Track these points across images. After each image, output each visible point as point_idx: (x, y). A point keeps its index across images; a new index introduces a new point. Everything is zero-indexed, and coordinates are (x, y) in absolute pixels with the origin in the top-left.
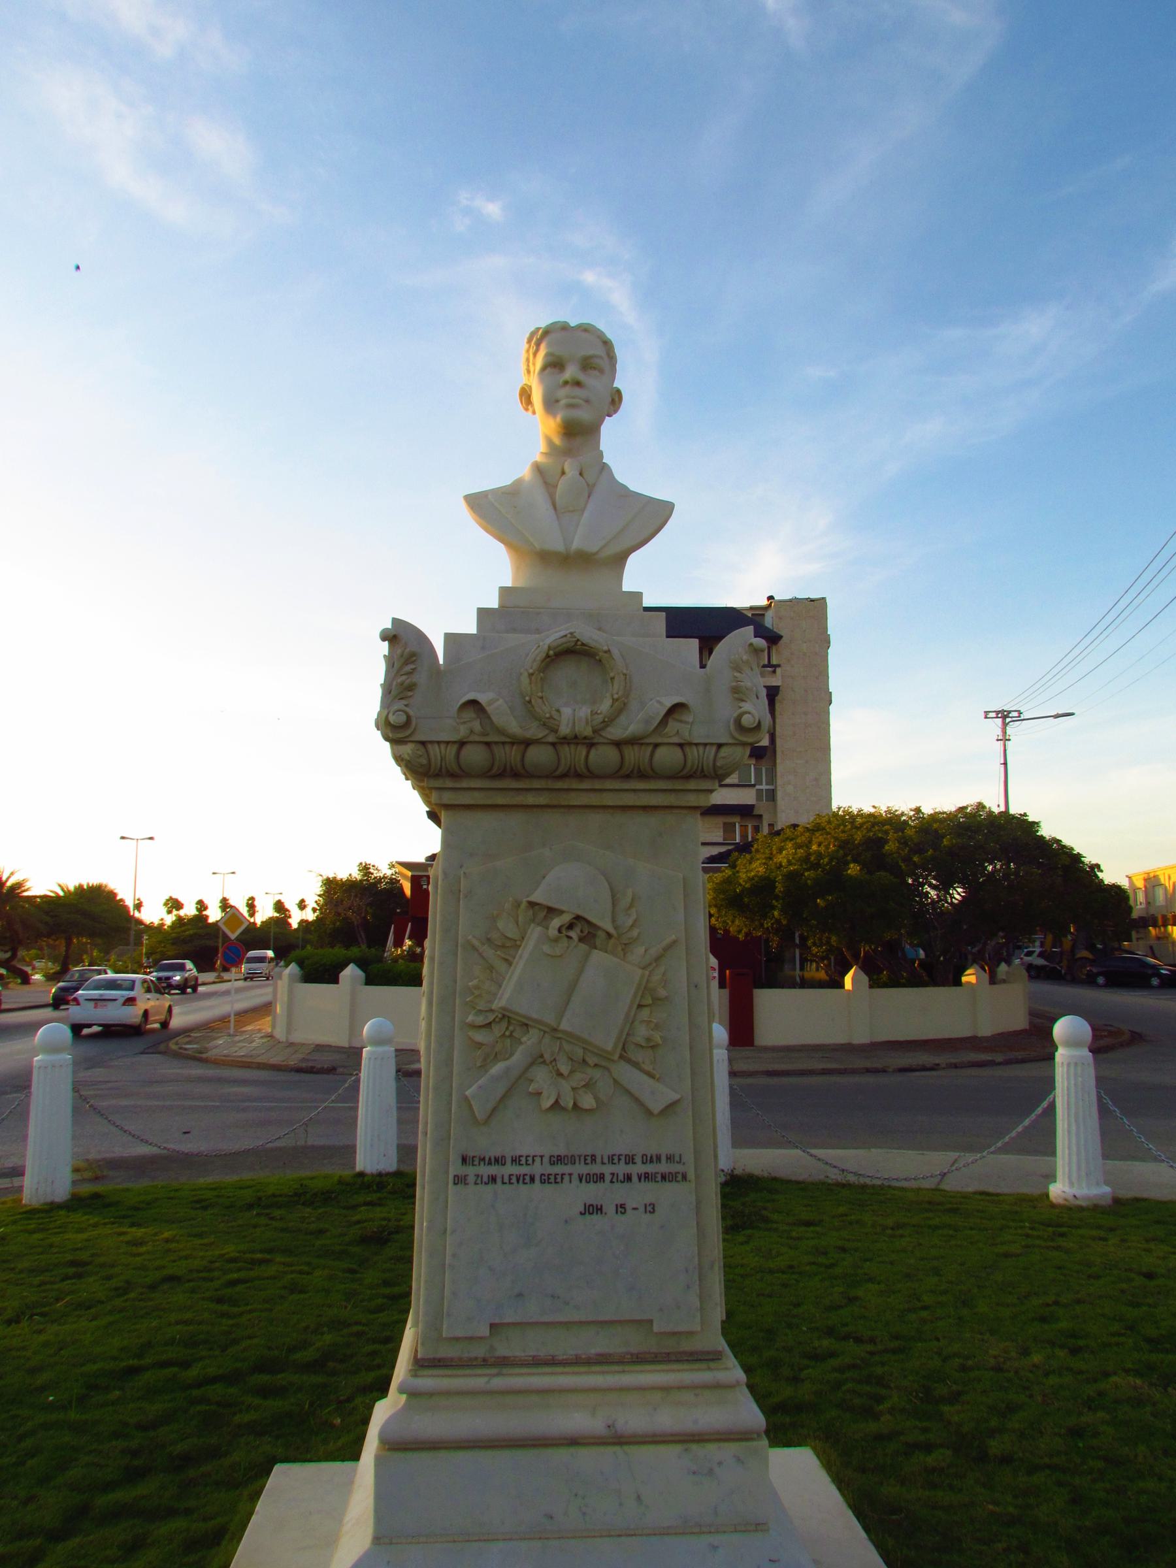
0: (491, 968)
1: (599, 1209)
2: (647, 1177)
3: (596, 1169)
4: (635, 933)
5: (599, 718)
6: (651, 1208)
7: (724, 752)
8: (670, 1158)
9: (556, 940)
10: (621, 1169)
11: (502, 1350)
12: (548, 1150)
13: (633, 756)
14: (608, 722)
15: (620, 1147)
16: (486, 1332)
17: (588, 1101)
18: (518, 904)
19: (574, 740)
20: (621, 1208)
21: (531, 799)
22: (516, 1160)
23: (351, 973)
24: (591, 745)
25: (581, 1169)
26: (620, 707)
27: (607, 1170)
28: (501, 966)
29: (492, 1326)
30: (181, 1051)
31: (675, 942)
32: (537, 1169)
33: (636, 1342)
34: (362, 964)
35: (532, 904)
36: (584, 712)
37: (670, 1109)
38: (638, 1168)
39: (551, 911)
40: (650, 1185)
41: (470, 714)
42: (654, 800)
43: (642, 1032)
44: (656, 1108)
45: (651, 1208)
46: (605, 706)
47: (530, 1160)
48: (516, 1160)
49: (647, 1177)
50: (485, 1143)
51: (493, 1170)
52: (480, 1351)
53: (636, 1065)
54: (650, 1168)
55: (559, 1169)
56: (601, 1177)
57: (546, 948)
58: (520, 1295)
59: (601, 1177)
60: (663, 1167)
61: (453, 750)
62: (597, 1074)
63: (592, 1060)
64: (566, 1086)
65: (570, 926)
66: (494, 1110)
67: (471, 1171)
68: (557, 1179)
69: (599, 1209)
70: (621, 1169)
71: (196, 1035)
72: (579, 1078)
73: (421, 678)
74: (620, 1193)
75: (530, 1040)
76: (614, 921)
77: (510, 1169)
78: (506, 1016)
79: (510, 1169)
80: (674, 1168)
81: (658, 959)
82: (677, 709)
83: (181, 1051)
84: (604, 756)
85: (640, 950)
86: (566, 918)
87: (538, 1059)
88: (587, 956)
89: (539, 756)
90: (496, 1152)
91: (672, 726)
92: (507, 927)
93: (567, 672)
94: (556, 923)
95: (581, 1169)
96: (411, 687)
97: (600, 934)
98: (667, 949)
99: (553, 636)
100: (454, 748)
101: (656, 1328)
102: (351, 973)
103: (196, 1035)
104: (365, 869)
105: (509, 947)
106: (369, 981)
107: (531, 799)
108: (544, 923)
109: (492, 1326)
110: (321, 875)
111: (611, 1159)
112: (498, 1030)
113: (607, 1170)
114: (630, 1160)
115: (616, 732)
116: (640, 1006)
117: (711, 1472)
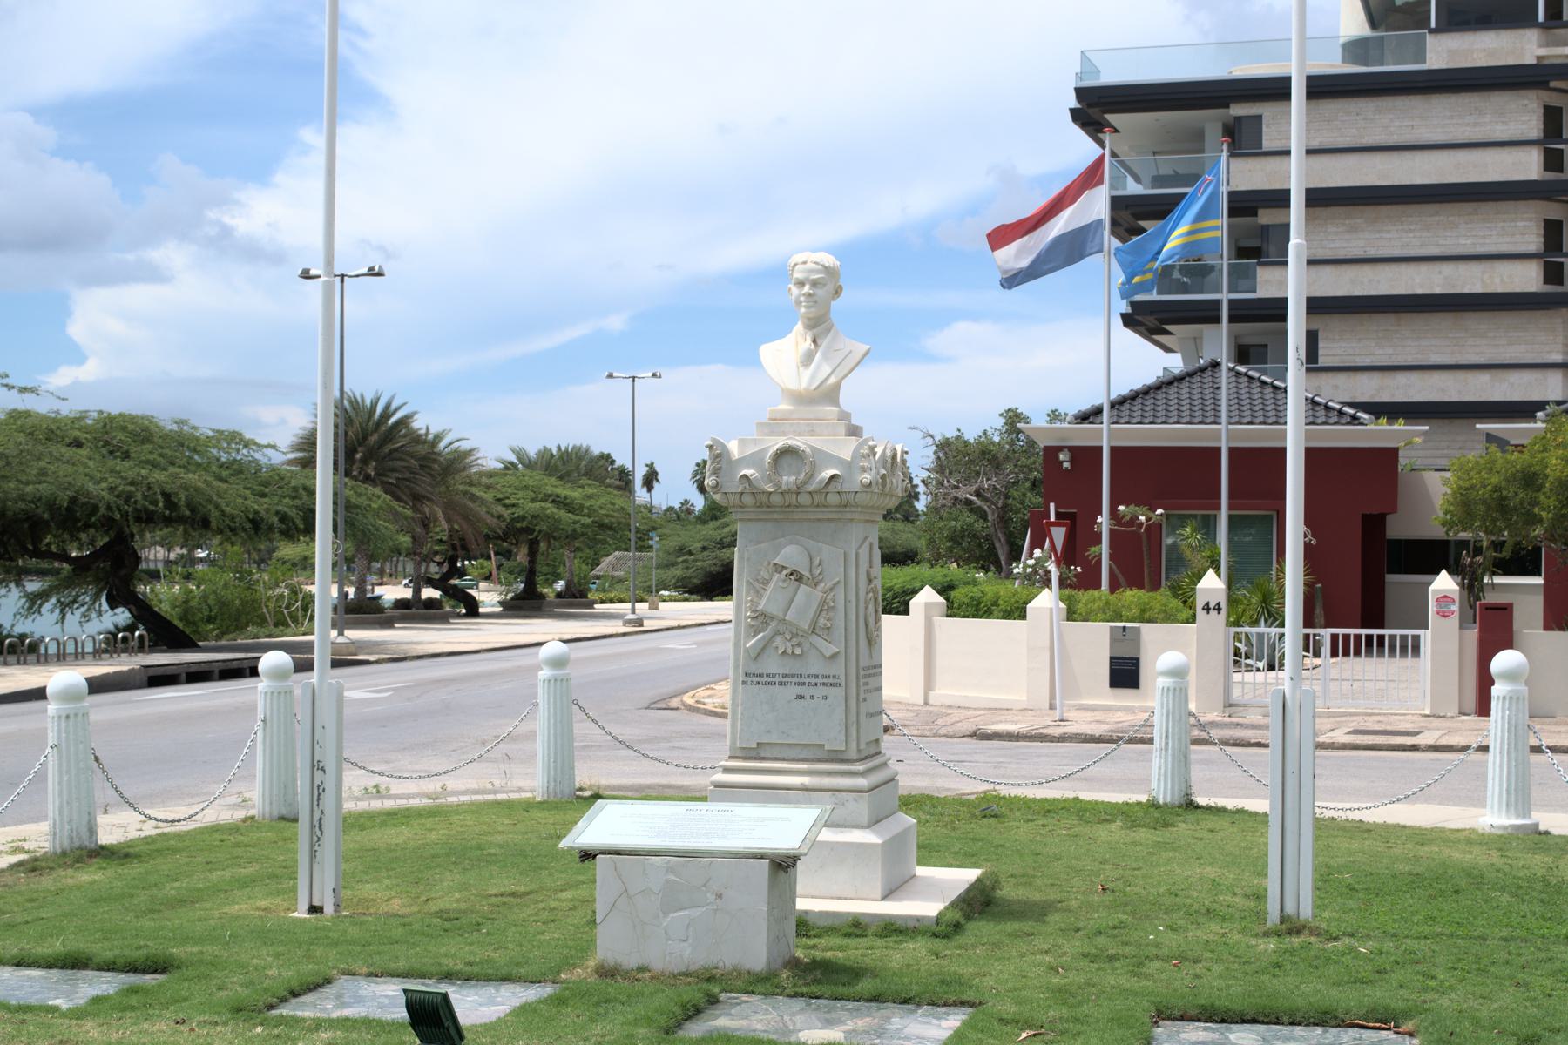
0: (758, 592)
1: (803, 697)
2: (824, 684)
3: (802, 680)
4: (821, 577)
5: (799, 481)
6: (825, 698)
7: (858, 495)
8: (834, 677)
9: (784, 581)
10: (813, 680)
11: (763, 755)
12: (782, 671)
13: (817, 498)
14: (805, 483)
15: (813, 672)
16: (755, 746)
17: (798, 651)
18: (769, 563)
19: (789, 491)
20: (812, 697)
21: (776, 516)
22: (768, 675)
23: (927, 597)
24: (798, 493)
25: (797, 680)
26: (811, 476)
27: (807, 681)
28: (762, 591)
29: (758, 744)
30: (699, 706)
31: (838, 582)
32: (777, 679)
33: (819, 754)
34: (944, 590)
35: (775, 564)
36: (792, 478)
37: (834, 656)
38: (820, 680)
39: (784, 568)
40: (824, 688)
41: (744, 480)
42: (831, 516)
43: (822, 621)
44: (828, 655)
45: (825, 698)
46: (802, 476)
47: (774, 675)
48: (768, 675)
49: (824, 684)
50: (753, 669)
51: (758, 679)
52: (754, 754)
53: (820, 636)
54: (825, 681)
55: (786, 679)
56: (804, 684)
57: (780, 584)
58: (769, 732)
59: (804, 684)
60: (831, 680)
61: (738, 496)
62: (803, 640)
63: (801, 633)
64: (789, 644)
65: (792, 574)
66: (759, 654)
67: (749, 679)
68: (785, 684)
69: (803, 697)
70: (813, 680)
71: (721, 688)
72: (795, 641)
73: (723, 464)
74: (812, 691)
75: (773, 624)
76: (811, 571)
77: (766, 679)
78: (763, 614)
79: (766, 679)
80: (836, 681)
81: (831, 589)
82: (833, 477)
83: (699, 706)
84: (804, 499)
85: (823, 585)
86: (789, 571)
87: (777, 633)
88: (798, 589)
89: (776, 499)
90: (760, 671)
91: (833, 484)
92: (764, 574)
93: (786, 461)
94: (785, 572)
95: (795, 680)
96: (719, 469)
97: (805, 578)
98: (835, 585)
99: (779, 442)
100: (738, 496)
101: (826, 748)
102: (927, 597)
103: (721, 688)
104: (1013, 419)
105: (766, 582)
106: (952, 611)
107: (776, 516)
108: (780, 573)
109: (758, 744)
110: (932, 436)
111: (809, 676)
112: (760, 620)
113: (807, 681)
114: (817, 677)
115: (811, 488)
116: (822, 610)
117: (843, 804)
